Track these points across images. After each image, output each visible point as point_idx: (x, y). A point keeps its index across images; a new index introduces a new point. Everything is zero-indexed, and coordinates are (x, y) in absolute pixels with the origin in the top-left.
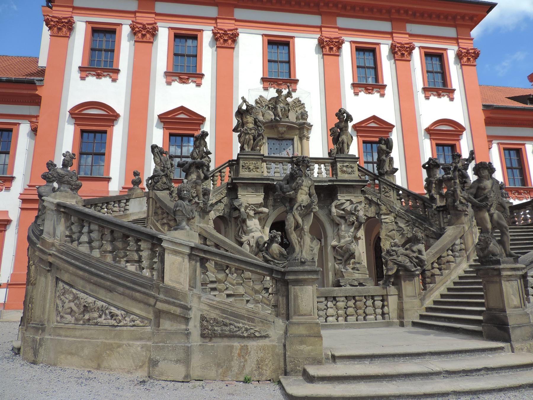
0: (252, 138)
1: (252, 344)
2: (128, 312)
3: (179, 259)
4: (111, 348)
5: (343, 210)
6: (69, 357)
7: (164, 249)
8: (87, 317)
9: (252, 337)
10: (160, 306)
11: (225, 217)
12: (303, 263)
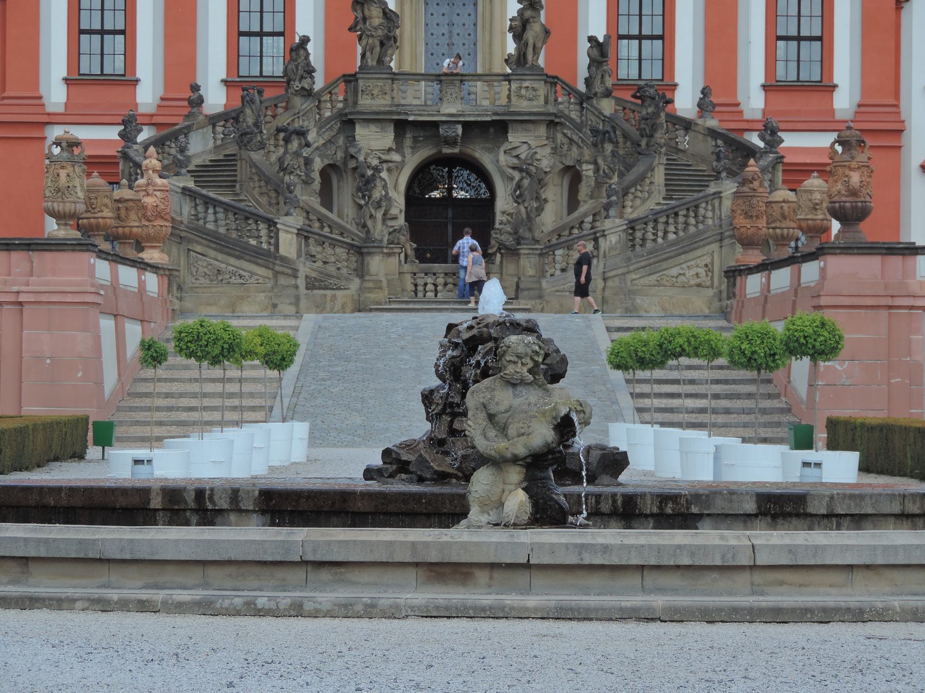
0: (378, 43)
1: (339, 293)
2: (252, 274)
3: (289, 236)
4: (242, 298)
5: (517, 157)
6: (209, 307)
7: (278, 230)
8: (220, 278)
9: (339, 289)
10: (277, 268)
11: (338, 166)
12: (374, 242)
